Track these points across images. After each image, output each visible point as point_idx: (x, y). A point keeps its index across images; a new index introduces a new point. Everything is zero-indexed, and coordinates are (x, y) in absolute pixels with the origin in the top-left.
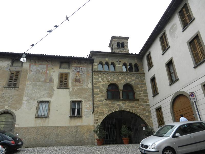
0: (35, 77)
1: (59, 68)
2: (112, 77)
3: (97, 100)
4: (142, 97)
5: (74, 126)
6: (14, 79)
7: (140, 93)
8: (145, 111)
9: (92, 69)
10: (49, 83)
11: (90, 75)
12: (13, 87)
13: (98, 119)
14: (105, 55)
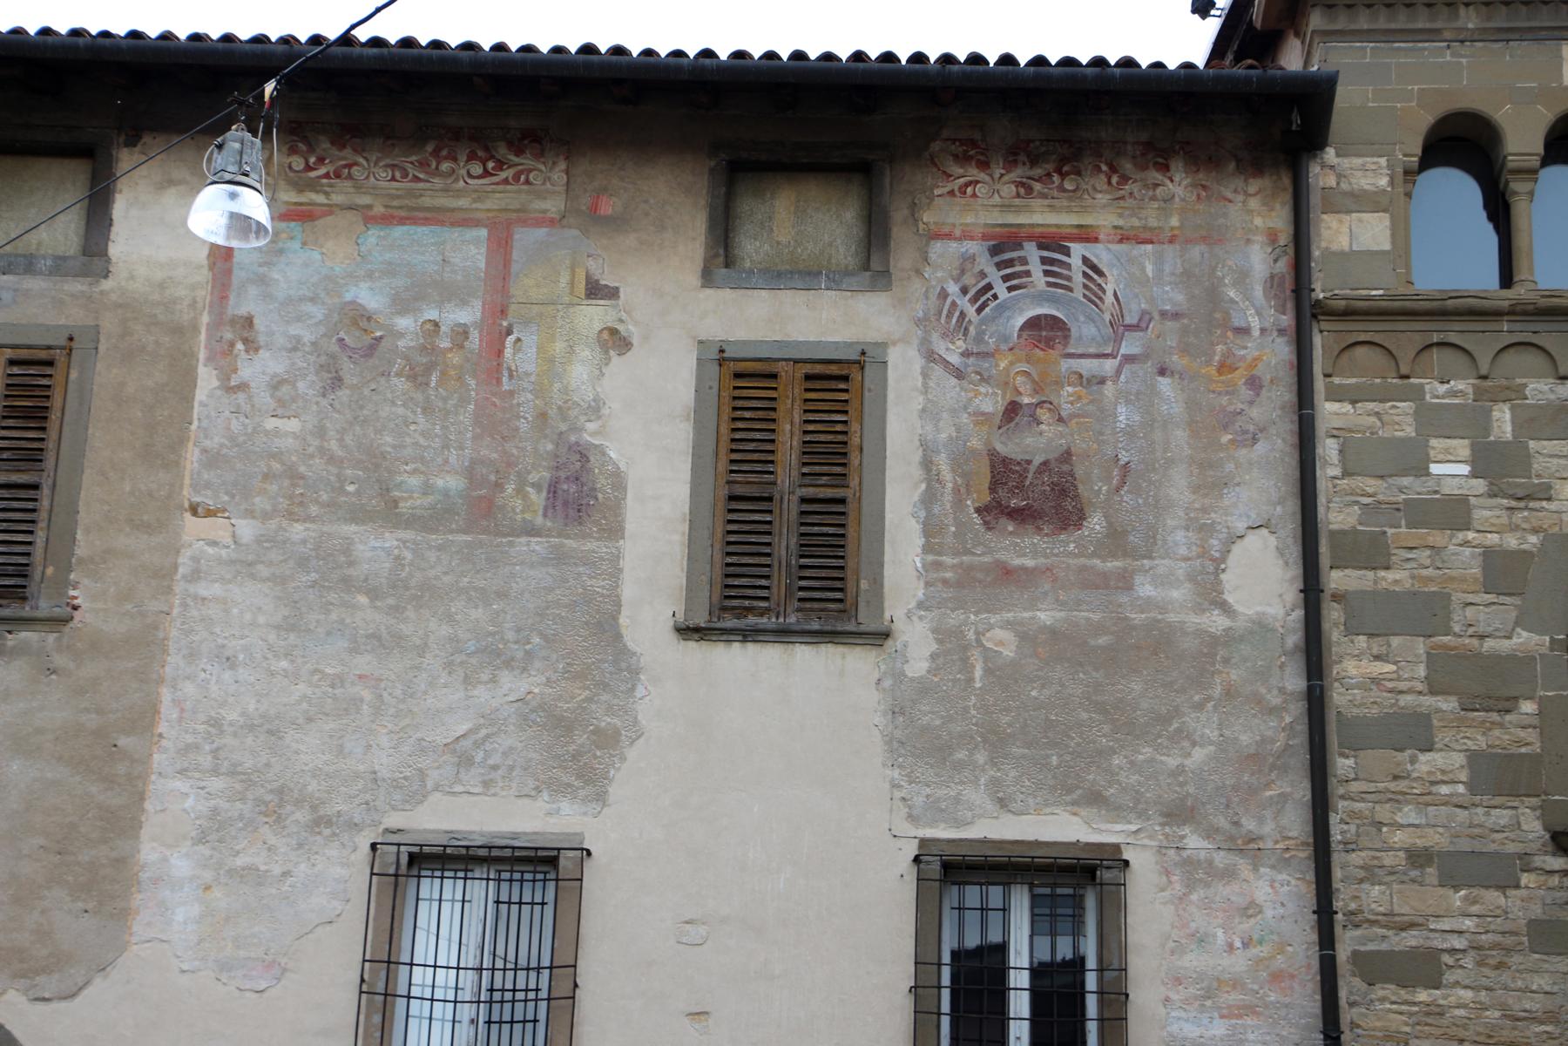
0: (321, 432)
1: (694, 279)
3: (1399, 838)
9: (1283, 266)
10: (538, 545)
11: (1254, 383)
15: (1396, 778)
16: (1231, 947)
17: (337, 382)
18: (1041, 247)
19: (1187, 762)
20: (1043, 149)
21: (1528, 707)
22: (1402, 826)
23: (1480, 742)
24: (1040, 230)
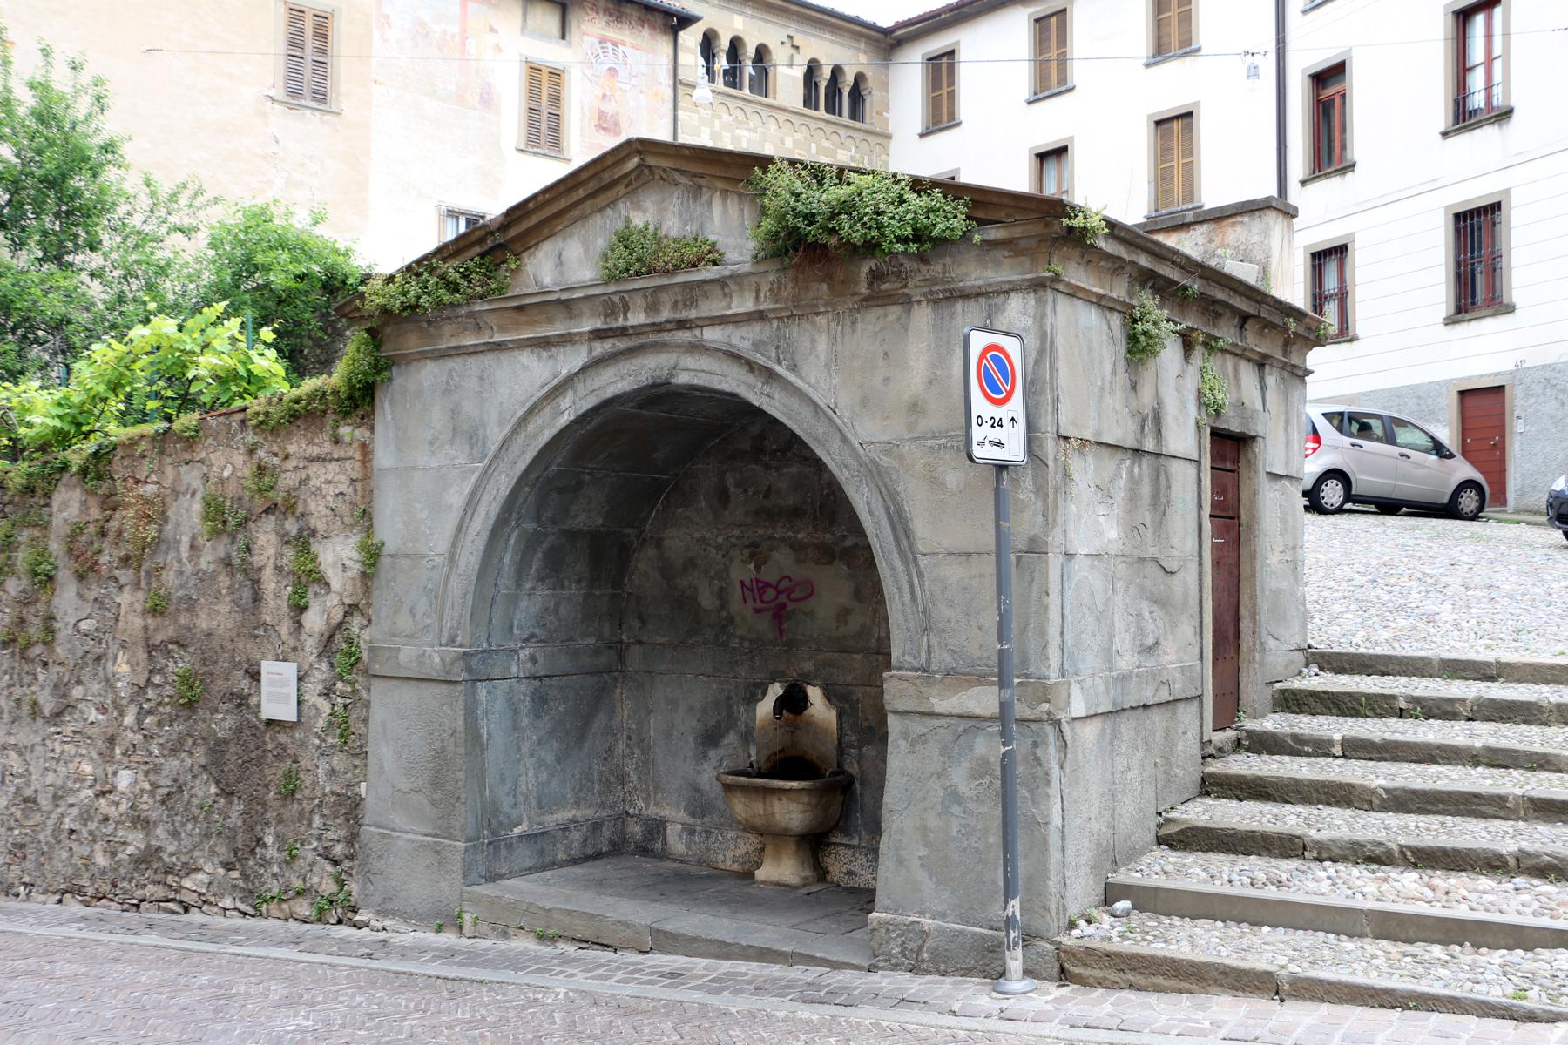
6: (309, 53)
11: (663, 100)
12: (314, 104)
17: (416, 45)
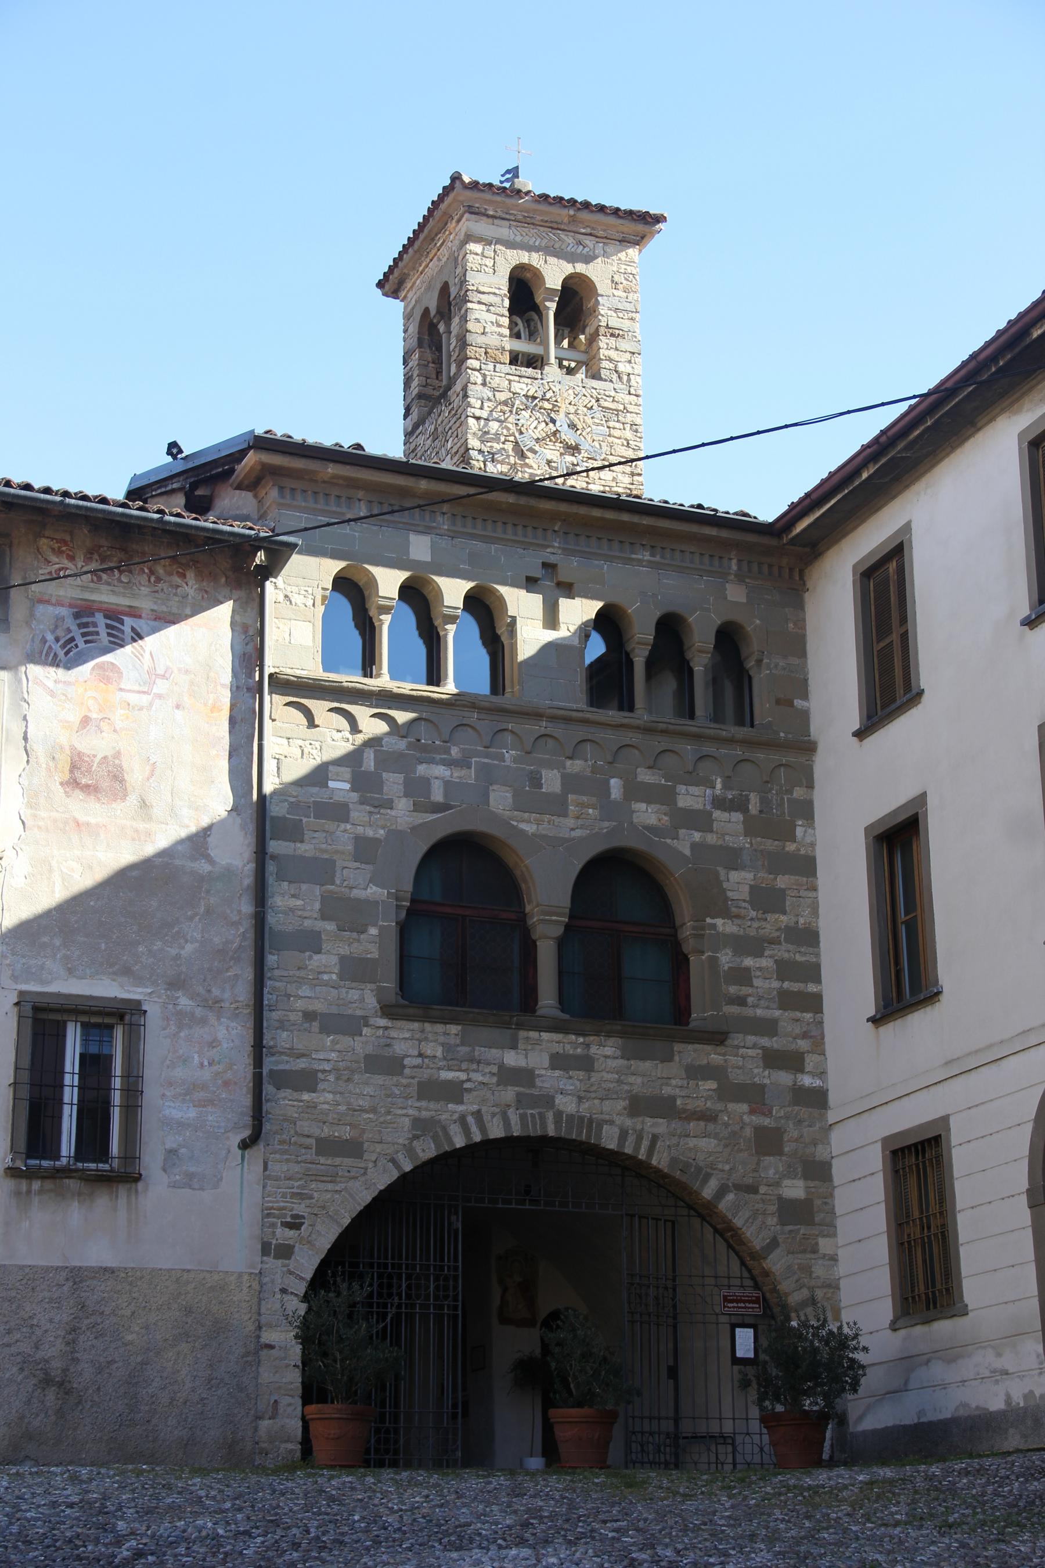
2: (462, 763)
3: (300, 1004)
4: (759, 1012)
5: (47, 1269)
7: (748, 962)
8: (780, 1153)
13: (300, 1209)
14: (403, 492)
15: (299, 969)
16: (202, 1065)
18: (106, 617)
19: (182, 952)
20: (109, 553)
21: (373, 931)
22: (302, 997)
23: (345, 950)
24: (106, 606)
